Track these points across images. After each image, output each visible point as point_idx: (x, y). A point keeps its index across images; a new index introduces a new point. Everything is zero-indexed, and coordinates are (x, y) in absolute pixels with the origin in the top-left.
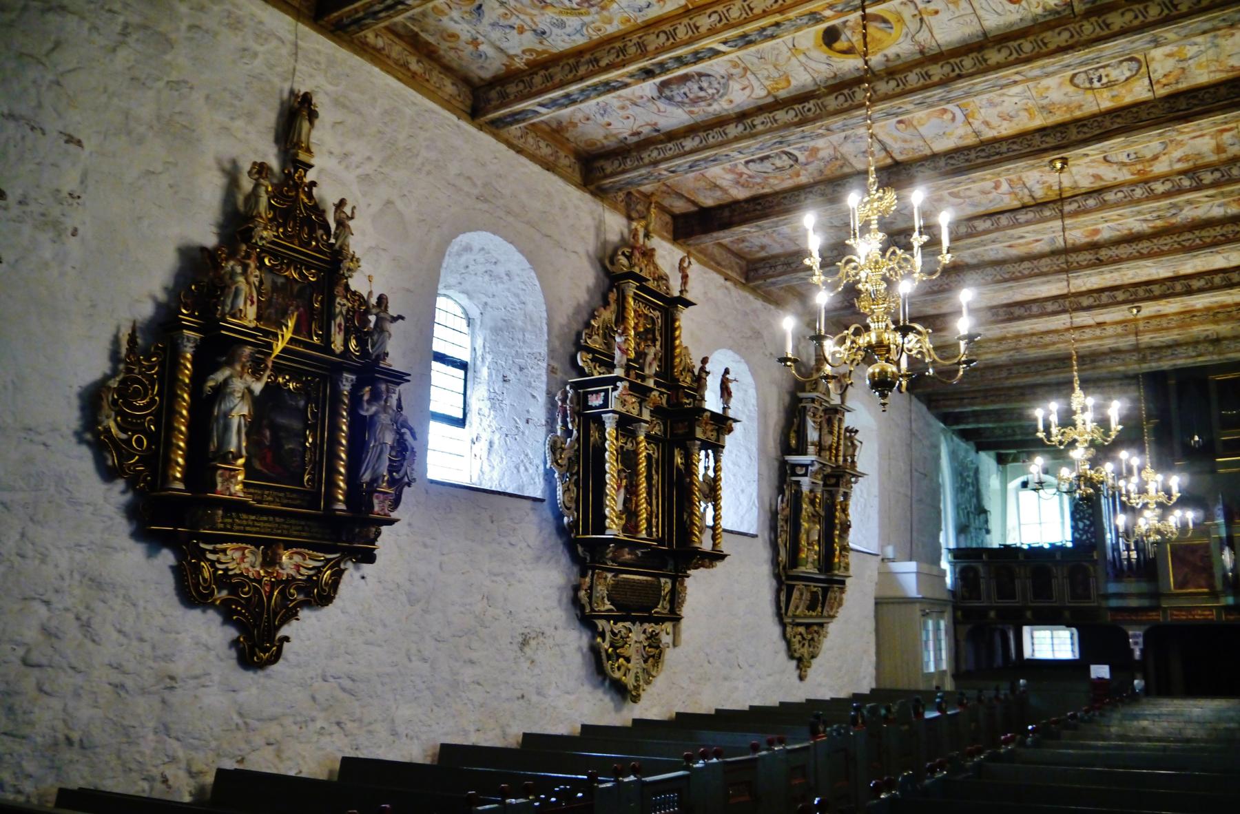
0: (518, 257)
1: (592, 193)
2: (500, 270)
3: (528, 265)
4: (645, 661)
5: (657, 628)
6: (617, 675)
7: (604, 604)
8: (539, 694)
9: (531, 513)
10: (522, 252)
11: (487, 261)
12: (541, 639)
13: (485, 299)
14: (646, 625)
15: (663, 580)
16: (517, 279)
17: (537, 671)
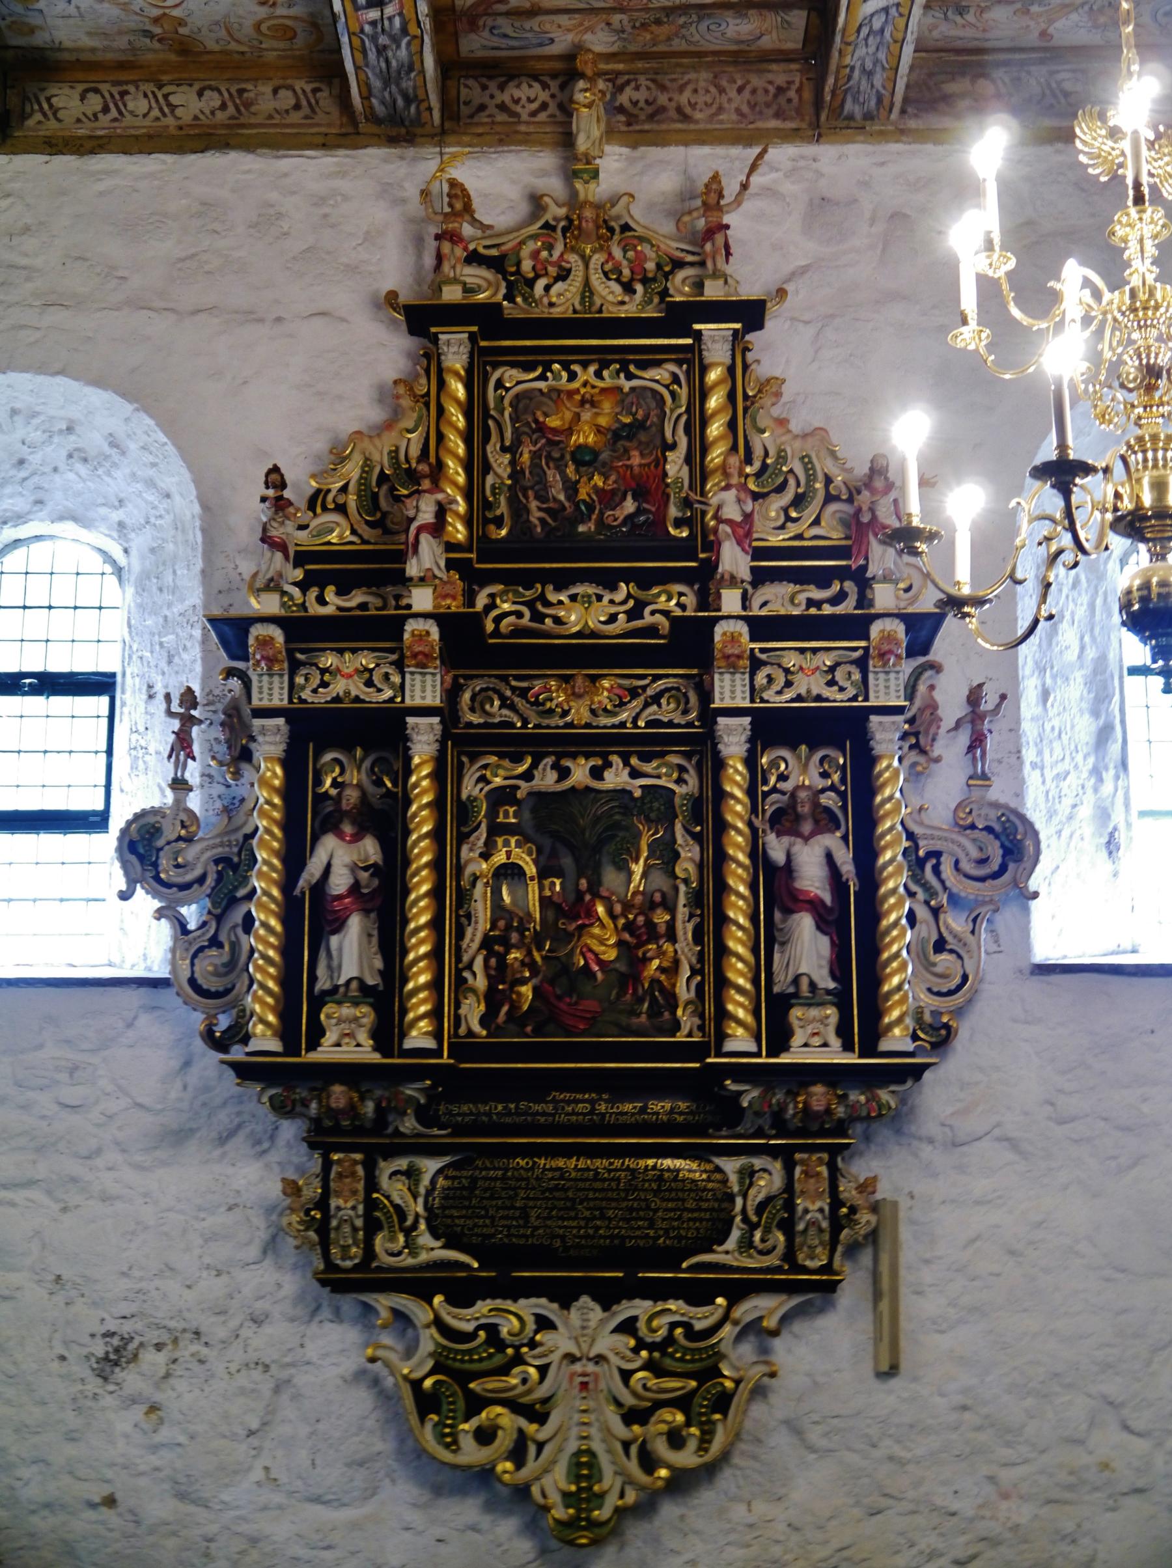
0: (97, 397)
1: (392, 141)
2: (94, 440)
3: (129, 408)
4: (632, 1417)
5: (702, 1317)
6: (471, 1453)
7: (411, 1247)
8: (182, 1496)
9: (144, 1019)
10: (98, 382)
11: (50, 434)
12: (190, 1348)
13: (116, 516)
14: (640, 1308)
15: (731, 1166)
16: (133, 446)
17: (165, 1434)
